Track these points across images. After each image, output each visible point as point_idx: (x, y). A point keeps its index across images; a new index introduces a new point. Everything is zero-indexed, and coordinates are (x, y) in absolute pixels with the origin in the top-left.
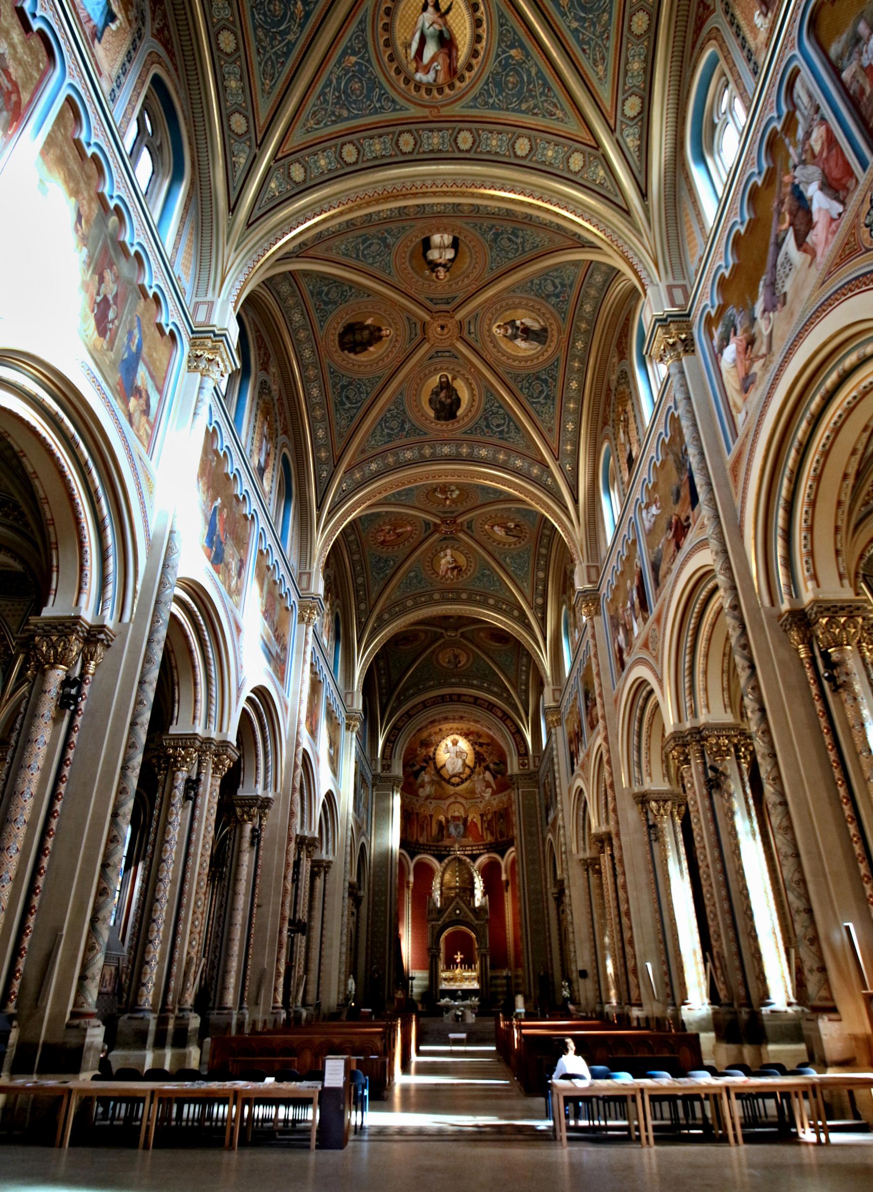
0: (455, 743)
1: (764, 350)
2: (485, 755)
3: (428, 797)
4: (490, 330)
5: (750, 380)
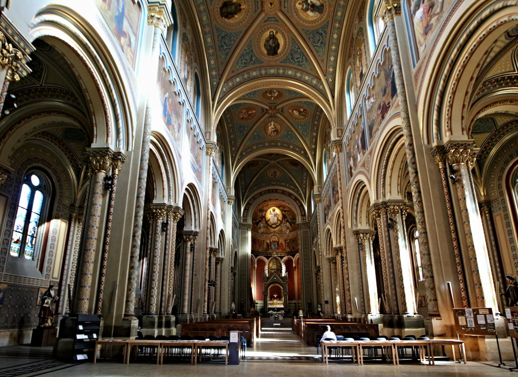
0: (274, 210)
1: (438, 10)
2: (287, 215)
3: (262, 233)
4: (295, 6)
5: (429, 28)
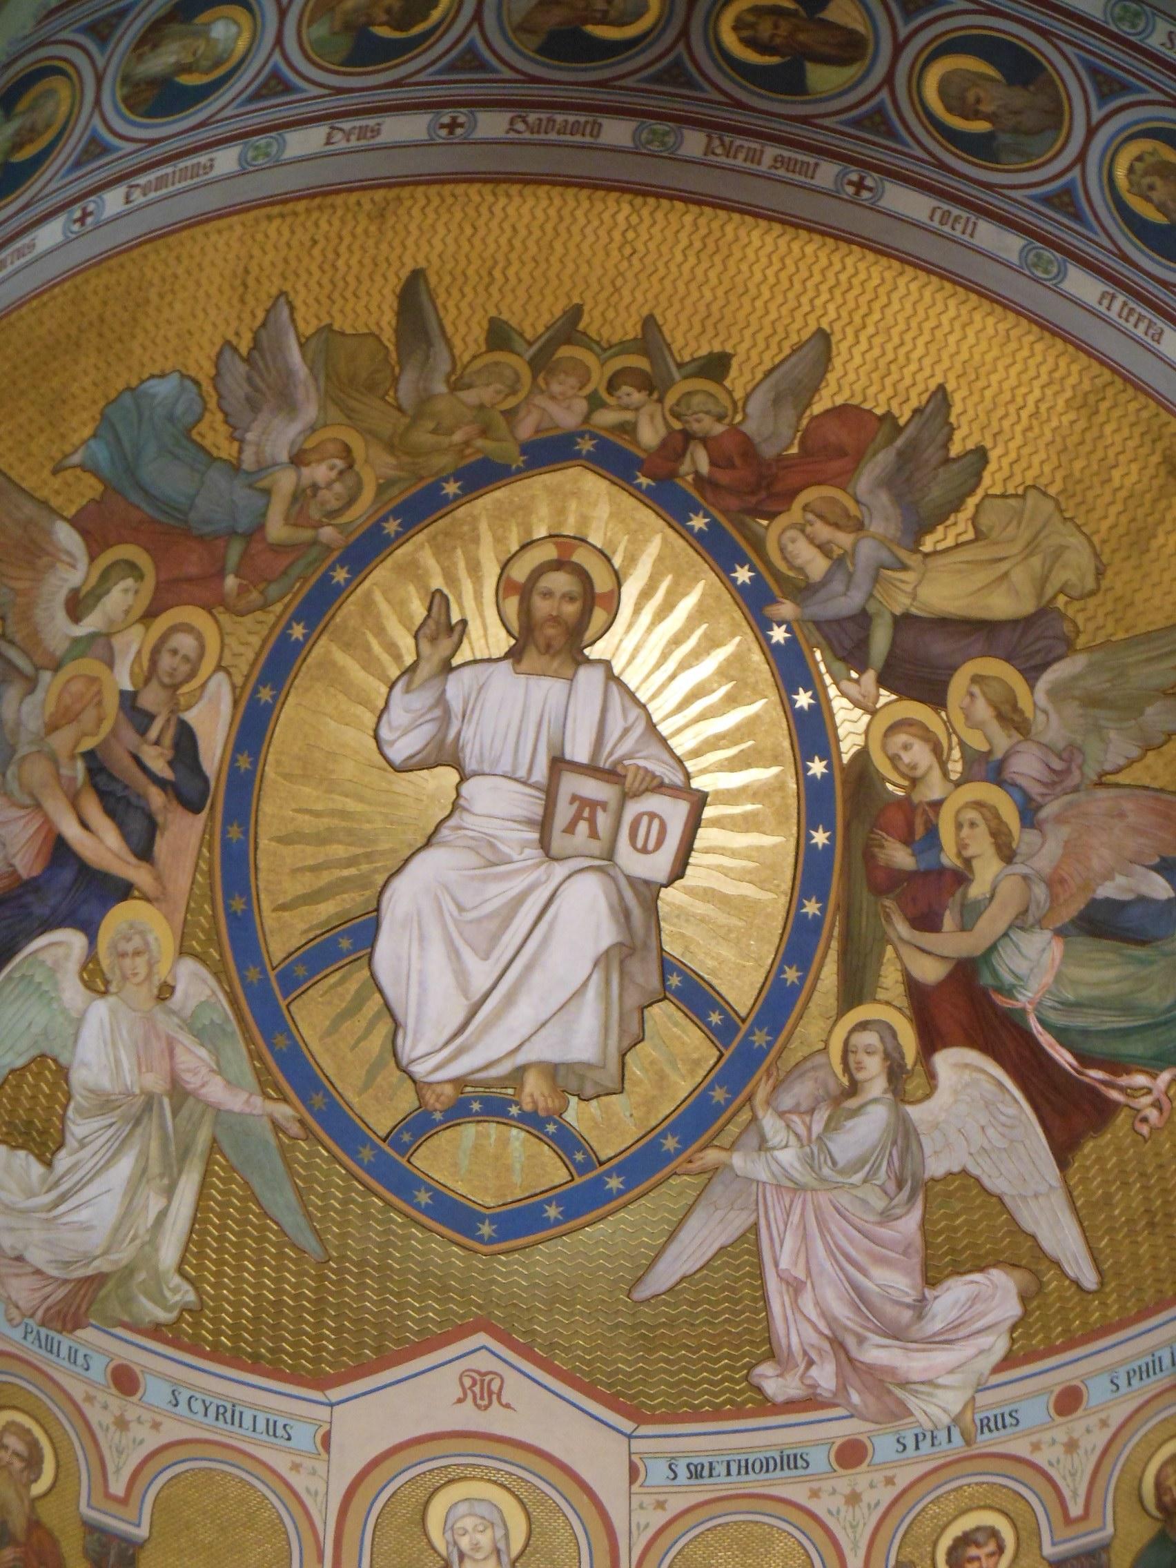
0: (559, 624)
2: (964, 823)
3: (80, 1301)
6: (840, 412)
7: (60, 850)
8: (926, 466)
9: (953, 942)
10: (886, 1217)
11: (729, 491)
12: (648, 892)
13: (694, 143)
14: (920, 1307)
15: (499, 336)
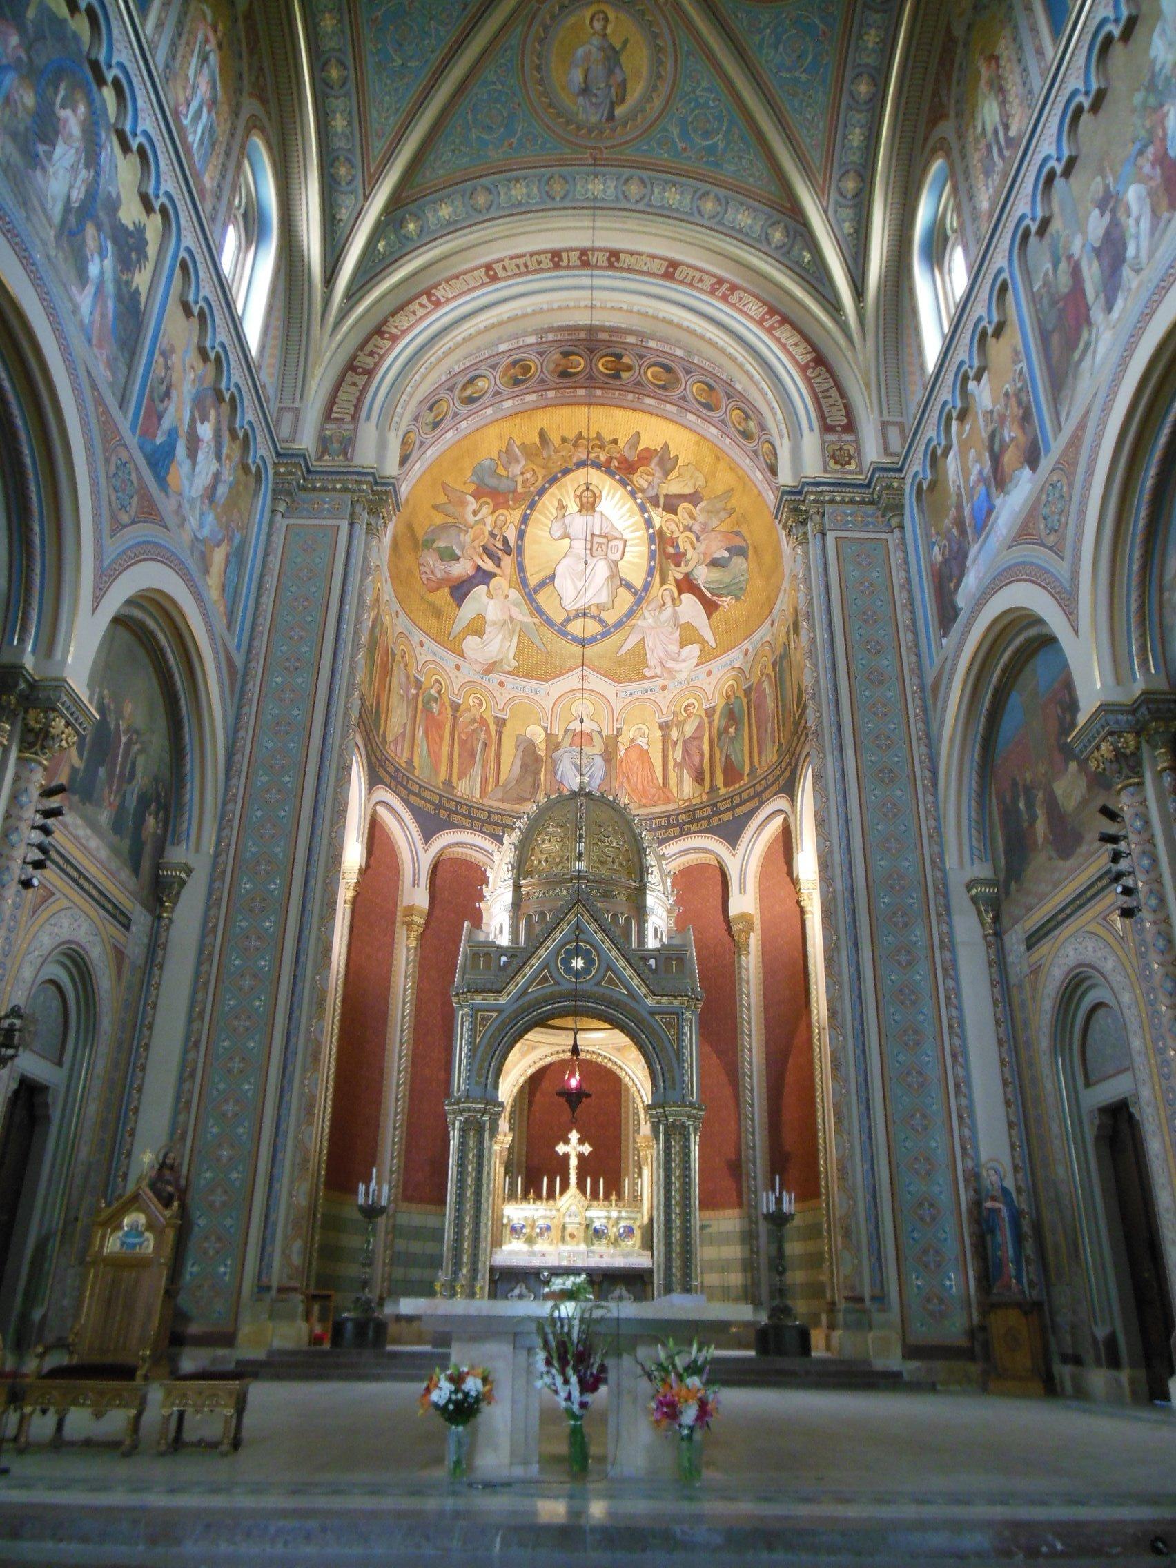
0: (588, 504)
3: (490, 669)
6: (646, 449)
7: (478, 568)
8: (666, 461)
9: (684, 569)
10: (672, 633)
11: (623, 469)
12: (616, 563)
13: (599, 392)
14: (679, 654)
15: (564, 440)
